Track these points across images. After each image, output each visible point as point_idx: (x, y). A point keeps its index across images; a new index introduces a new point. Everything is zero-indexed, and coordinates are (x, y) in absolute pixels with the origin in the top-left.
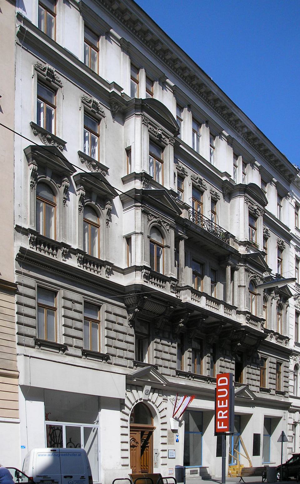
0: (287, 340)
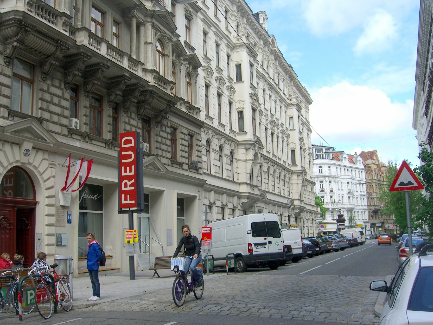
0: (198, 111)
